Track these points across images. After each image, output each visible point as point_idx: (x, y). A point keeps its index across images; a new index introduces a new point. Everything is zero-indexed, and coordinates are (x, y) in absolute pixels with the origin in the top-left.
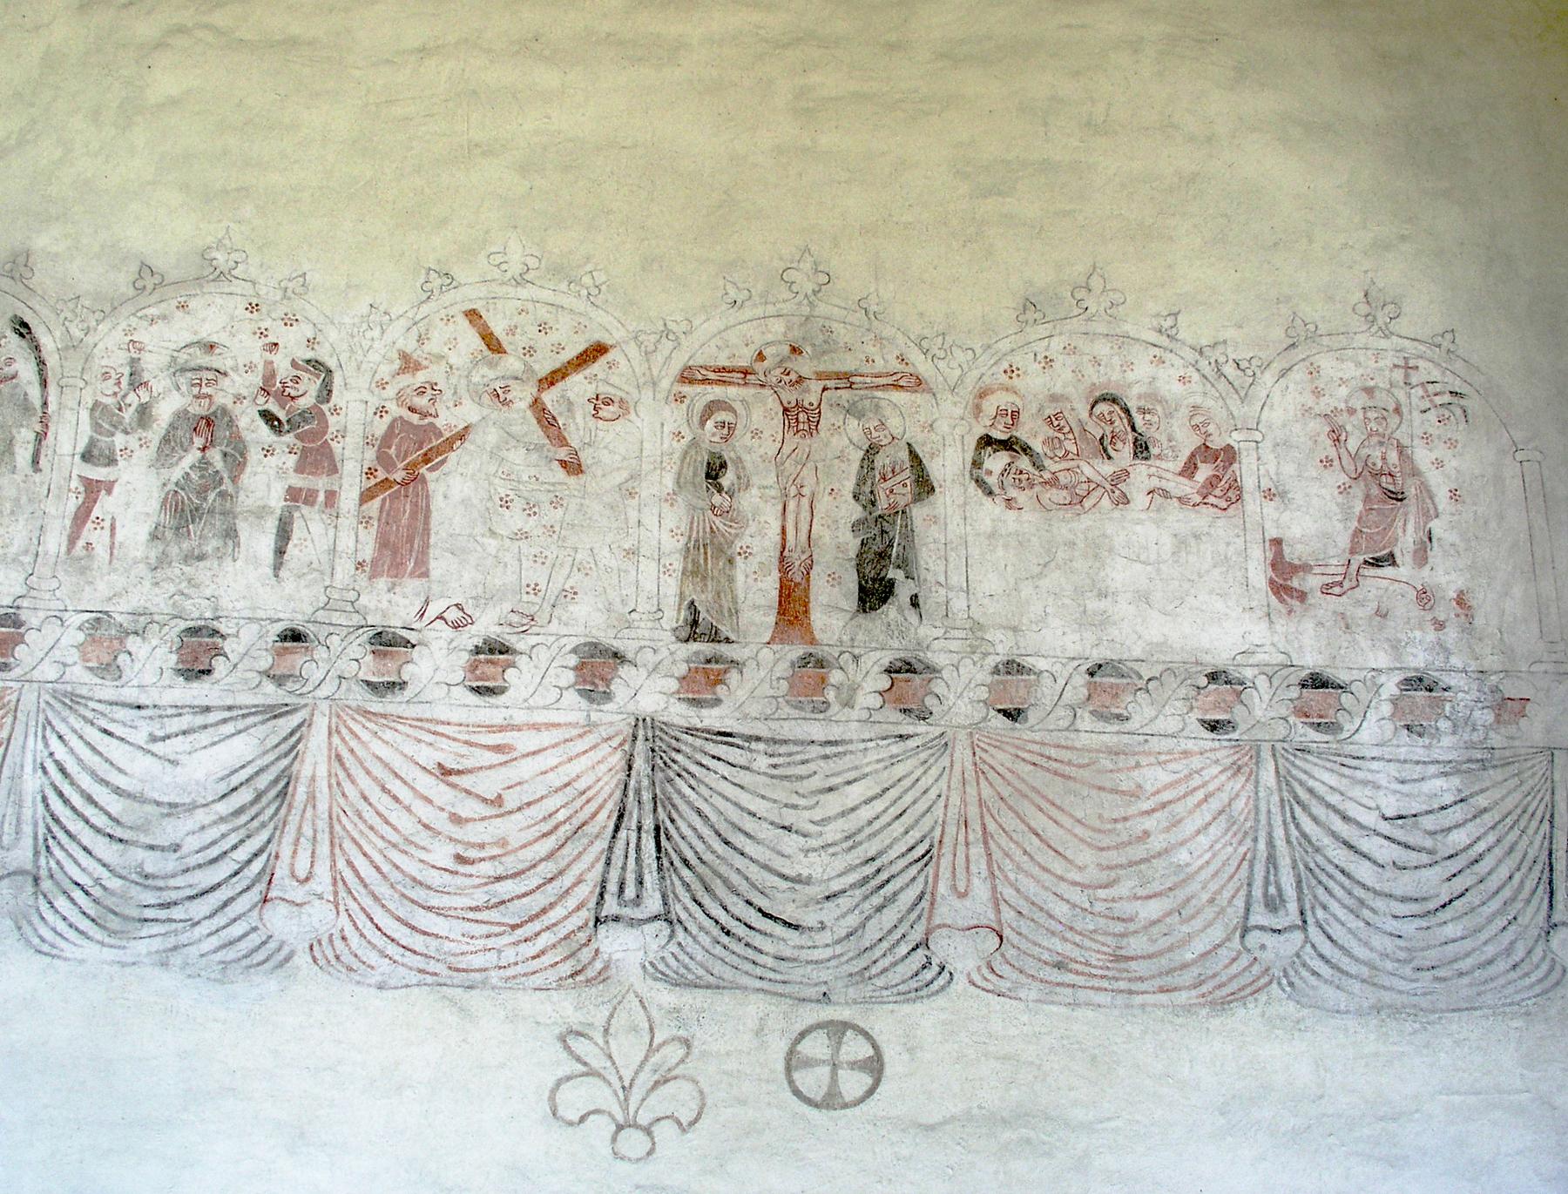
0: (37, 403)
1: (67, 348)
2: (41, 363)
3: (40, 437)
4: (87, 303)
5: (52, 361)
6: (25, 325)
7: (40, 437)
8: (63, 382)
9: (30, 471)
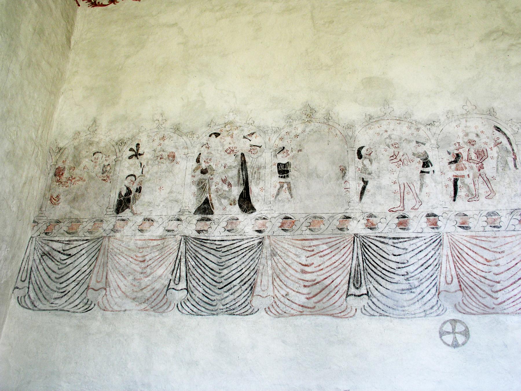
0: (511, 150)
1: (514, 134)
2: (508, 138)
3: (515, 159)
4: (515, 121)
5: (511, 138)
6: (499, 128)
7: (515, 159)
8: (517, 143)
9: (515, 169)
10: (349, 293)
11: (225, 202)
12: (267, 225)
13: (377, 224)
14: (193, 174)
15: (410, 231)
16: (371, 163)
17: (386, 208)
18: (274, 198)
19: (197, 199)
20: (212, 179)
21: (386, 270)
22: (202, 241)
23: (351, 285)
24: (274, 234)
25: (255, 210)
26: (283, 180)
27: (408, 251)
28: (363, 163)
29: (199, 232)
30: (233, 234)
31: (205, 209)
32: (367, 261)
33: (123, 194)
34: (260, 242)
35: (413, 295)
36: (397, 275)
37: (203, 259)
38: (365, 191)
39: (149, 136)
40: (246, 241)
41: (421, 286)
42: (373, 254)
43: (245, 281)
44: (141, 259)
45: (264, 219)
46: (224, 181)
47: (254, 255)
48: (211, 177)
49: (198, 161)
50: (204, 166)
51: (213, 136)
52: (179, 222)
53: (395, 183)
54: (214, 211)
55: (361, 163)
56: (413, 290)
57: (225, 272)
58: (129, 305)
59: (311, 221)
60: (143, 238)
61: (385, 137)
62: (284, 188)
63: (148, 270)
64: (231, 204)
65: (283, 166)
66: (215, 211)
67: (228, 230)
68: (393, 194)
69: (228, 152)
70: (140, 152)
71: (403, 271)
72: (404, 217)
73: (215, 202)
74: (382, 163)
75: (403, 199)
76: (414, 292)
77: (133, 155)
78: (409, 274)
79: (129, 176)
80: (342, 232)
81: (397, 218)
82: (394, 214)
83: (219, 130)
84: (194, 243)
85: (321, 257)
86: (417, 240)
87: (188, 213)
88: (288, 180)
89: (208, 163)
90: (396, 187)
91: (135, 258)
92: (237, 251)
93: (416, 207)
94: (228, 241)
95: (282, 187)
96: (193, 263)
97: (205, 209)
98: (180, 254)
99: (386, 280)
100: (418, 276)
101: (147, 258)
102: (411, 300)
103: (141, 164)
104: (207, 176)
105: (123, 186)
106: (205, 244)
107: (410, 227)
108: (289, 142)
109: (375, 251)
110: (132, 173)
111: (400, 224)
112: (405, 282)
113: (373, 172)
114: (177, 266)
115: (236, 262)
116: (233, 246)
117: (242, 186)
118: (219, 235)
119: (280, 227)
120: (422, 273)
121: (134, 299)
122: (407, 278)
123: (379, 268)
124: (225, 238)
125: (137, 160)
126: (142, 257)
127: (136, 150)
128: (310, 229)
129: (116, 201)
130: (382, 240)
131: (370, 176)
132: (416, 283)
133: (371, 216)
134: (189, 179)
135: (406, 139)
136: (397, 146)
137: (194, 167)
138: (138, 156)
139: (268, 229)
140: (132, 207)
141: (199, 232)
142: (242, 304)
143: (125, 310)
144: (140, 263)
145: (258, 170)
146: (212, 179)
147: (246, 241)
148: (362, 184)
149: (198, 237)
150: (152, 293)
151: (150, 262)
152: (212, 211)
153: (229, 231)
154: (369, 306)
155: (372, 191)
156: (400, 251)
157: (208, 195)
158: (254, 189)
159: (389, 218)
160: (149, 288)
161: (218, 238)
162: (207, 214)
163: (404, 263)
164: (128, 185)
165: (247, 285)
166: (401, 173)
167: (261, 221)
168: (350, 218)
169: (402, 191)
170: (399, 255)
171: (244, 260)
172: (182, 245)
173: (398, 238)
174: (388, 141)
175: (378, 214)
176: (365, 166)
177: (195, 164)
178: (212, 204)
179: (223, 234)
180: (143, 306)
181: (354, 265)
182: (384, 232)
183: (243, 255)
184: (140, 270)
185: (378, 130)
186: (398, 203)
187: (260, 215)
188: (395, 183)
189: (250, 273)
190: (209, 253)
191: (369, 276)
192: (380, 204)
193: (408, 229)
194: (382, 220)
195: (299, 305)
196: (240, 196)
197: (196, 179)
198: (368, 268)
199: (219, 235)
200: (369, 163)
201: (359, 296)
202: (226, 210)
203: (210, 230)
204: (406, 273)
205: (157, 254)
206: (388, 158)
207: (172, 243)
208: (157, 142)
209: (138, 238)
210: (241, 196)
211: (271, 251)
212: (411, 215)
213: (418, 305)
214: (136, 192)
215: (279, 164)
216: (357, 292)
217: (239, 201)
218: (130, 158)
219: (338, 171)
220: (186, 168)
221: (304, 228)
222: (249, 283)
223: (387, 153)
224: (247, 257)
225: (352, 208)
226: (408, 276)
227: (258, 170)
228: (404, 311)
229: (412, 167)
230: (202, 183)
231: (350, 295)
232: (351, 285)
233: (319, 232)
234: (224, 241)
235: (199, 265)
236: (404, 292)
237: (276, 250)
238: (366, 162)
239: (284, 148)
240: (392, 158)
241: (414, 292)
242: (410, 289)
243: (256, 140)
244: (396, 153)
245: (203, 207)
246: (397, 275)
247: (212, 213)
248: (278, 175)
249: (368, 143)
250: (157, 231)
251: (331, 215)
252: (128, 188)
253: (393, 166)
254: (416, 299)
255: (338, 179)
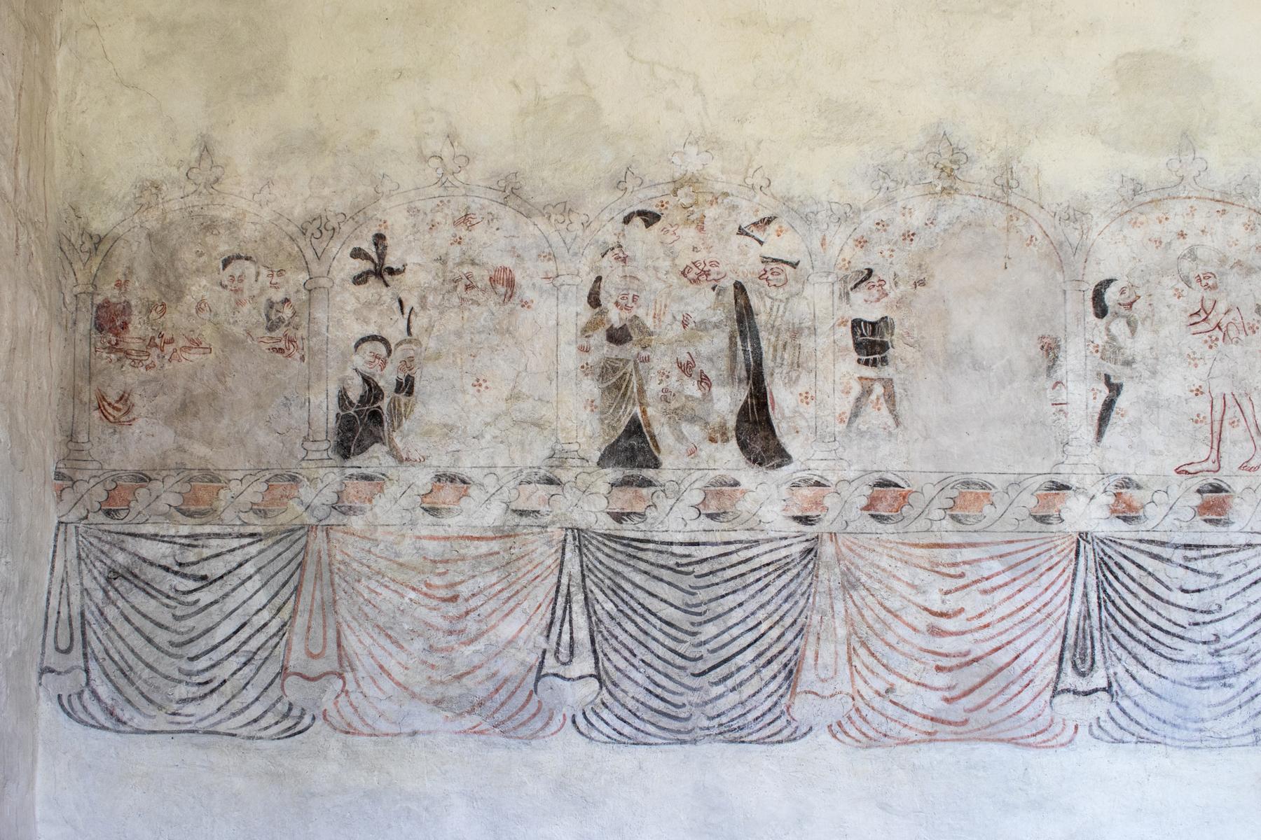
10: (1060, 687)
11: (693, 432)
12: (827, 502)
13: (1143, 507)
14: (584, 342)
15: (1232, 528)
16: (1133, 332)
17: (1170, 465)
18: (845, 425)
19: (602, 421)
20: (647, 360)
21: (1161, 629)
22: (629, 545)
23: (1067, 666)
24: (849, 529)
25: (789, 457)
26: (869, 372)
27: (1223, 581)
28: (1108, 330)
29: (619, 517)
30: (725, 526)
31: (633, 450)
32: (1109, 605)
33: (355, 394)
34: (809, 551)
35: (1229, 693)
36: (1191, 641)
37: (639, 594)
38: (1113, 414)
39: (413, 211)
40: (767, 547)
41: (1252, 670)
42: (1127, 588)
43: (769, 655)
44: (443, 593)
45: (818, 484)
46: (686, 368)
47: (793, 586)
48: (644, 354)
49: (594, 300)
50: (615, 317)
51: (638, 221)
52: (553, 489)
53: (1198, 392)
54: (661, 457)
55: (1102, 328)
56: (1228, 681)
57: (710, 630)
58: (425, 718)
59: (955, 493)
60: (441, 532)
61: (1179, 253)
62: (873, 397)
63: (471, 625)
64: (712, 440)
65: (869, 328)
66: (666, 460)
67: (708, 516)
68: (1192, 424)
69: (692, 275)
70: (392, 260)
71: (1206, 633)
72: (1217, 489)
73: (662, 430)
74: (1164, 332)
75: (1217, 440)
76: (1230, 686)
77: (368, 273)
78: (1222, 639)
79: (363, 340)
80: (1044, 527)
81: (1199, 491)
82: (1189, 482)
83: (656, 202)
84: (606, 550)
85: (985, 592)
86: (1251, 552)
87: (578, 462)
88: (887, 372)
89: (627, 308)
90: (1202, 406)
91: (425, 589)
92: (742, 575)
93: (1253, 463)
94: (713, 544)
95: (867, 392)
96: (609, 606)
97: (633, 450)
98: (565, 580)
99: (1161, 655)
100: (1244, 645)
101: (464, 590)
102: (1220, 704)
103: (401, 302)
104: (630, 350)
105: (350, 372)
106: (640, 554)
107: (1233, 517)
108: (887, 253)
109: (1133, 580)
110: (372, 330)
111: (1204, 508)
112: (1209, 659)
113: (1138, 358)
114: (559, 613)
115: (740, 605)
116: (726, 561)
117: (744, 385)
118: (681, 527)
119: (866, 508)
120: (1255, 639)
121: (437, 703)
122: (1217, 651)
123: (1142, 624)
124: (702, 538)
125: (385, 290)
126: (446, 587)
127: (374, 256)
128: (953, 517)
129: (332, 418)
130: (1156, 550)
131: (1127, 371)
132: (1239, 663)
133: (1127, 483)
134: (570, 358)
135: (1239, 263)
136: (1210, 282)
137: (584, 320)
138: (387, 277)
139: (831, 515)
140: (391, 440)
141: (619, 517)
142: (764, 714)
143: (415, 733)
144: (443, 605)
145: (794, 337)
146: (647, 360)
147: (767, 547)
148: (1104, 393)
149: (618, 533)
150: (491, 686)
151: (473, 603)
152: (656, 458)
153: (711, 516)
154: (1112, 719)
155: (1132, 414)
156: (1204, 581)
157: (637, 410)
158: (783, 398)
159: (1175, 492)
160: (481, 674)
161: (680, 538)
162: (641, 466)
163: (1209, 612)
164: (366, 369)
165: (775, 666)
166: (1218, 365)
167: (807, 492)
168: (1068, 488)
169: (1217, 416)
170: (1199, 591)
171: (763, 598)
172: (568, 555)
173: (1199, 547)
174: (1186, 265)
175: (1145, 479)
176: (1113, 338)
177: (587, 313)
178: (653, 437)
179: (693, 525)
180: (468, 722)
181: (1074, 616)
182: (1159, 528)
183: (761, 584)
184: (445, 625)
185: (1156, 230)
186: (1204, 451)
187: (805, 475)
188: (1198, 392)
189: (783, 634)
190: (655, 577)
191: (1114, 645)
192: (1153, 453)
193: (1227, 523)
194: (1157, 497)
195: (925, 717)
196: (739, 414)
197: (592, 358)
198: (1111, 623)
199: (681, 527)
200: (1127, 330)
201: (1086, 694)
202: (697, 458)
203: (651, 513)
204: (1213, 638)
205: (493, 578)
206: (1184, 318)
207: (540, 550)
208: (446, 232)
209: (425, 532)
210: (743, 414)
211: (843, 573)
212: (1237, 484)
213: (1238, 716)
214: (398, 390)
215: (856, 324)
216: (1082, 685)
217: (737, 429)
218: (360, 279)
219: (1035, 351)
220: (555, 317)
221: (936, 514)
222: (783, 659)
223: (1181, 303)
224: (772, 590)
225: (1072, 460)
226: (1218, 646)
227: (794, 337)
228: (1201, 730)
229: (1251, 349)
230: (615, 370)
231: (1063, 691)
232: (1067, 666)
233: (978, 527)
234: (698, 544)
235: (630, 612)
236: (1205, 685)
237: (858, 573)
238: (1119, 328)
239: (870, 272)
240: (1196, 319)
241: (1230, 686)
242: (1221, 679)
243: (779, 244)
244: (1208, 305)
245: (624, 444)
246: (1191, 641)
247: (657, 465)
248: (855, 356)
249: (1127, 271)
250: (481, 512)
251: (1012, 478)
252: (366, 380)
253: (1197, 343)
254: (1235, 703)
255: (1034, 376)
